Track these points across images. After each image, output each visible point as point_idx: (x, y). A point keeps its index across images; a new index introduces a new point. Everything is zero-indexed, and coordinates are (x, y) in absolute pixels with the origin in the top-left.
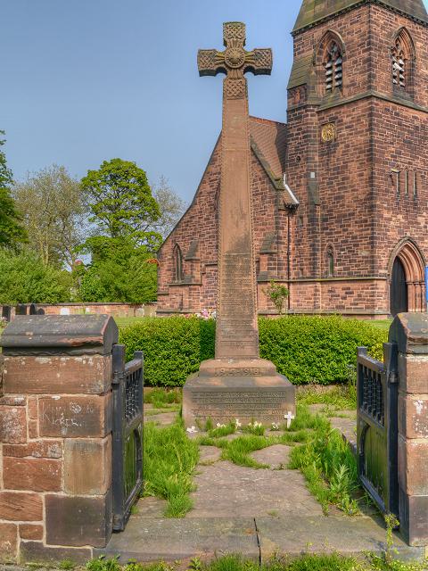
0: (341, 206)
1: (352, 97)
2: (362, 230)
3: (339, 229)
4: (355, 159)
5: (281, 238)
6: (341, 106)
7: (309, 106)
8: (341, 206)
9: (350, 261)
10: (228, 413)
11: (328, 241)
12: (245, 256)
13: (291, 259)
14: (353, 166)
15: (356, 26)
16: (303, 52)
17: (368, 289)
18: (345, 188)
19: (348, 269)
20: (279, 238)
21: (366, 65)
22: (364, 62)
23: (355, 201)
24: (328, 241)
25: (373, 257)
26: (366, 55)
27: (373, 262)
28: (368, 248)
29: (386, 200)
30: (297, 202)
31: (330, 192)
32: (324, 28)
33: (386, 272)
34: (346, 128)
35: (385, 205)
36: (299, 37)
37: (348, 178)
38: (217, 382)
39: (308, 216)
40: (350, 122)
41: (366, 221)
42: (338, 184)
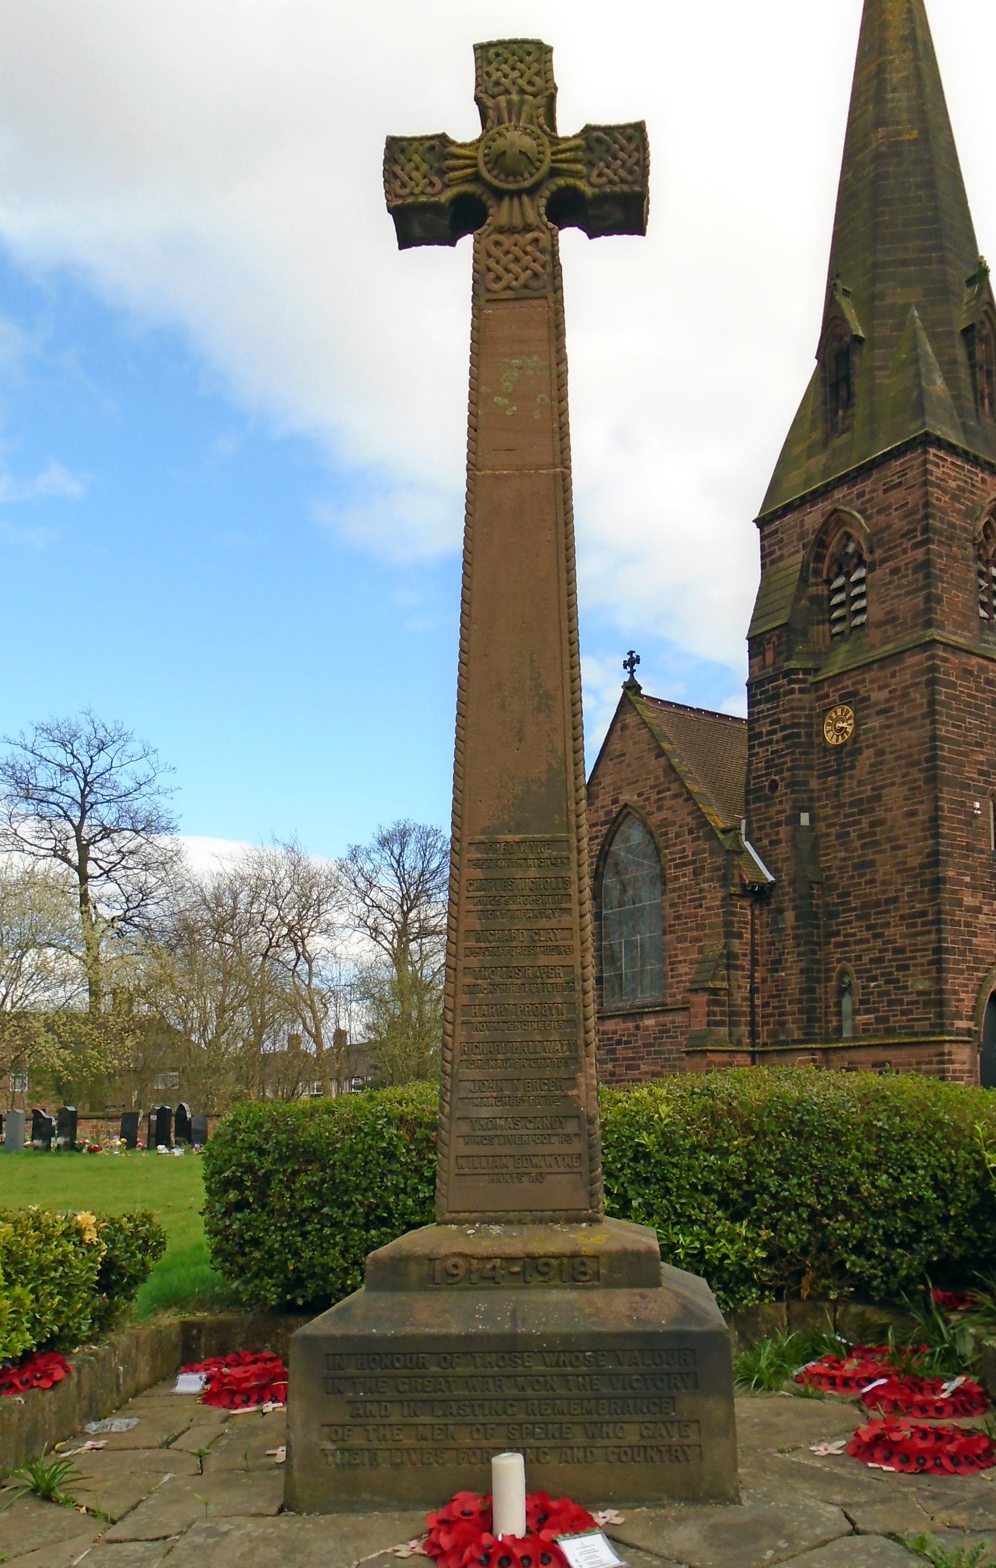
0: (867, 883)
1: (889, 647)
2: (916, 935)
3: (866, 934)
4: (898, 780)
5: (736, 956)
6: (866, 667)
7: (795, 671)
8: (867, 883)
9: (890, 1003)
10: (465, 1440)
11: (839, 961)
12: (548, 843)
13: (757, 1002)
14: (894, 795)
15: (895, 497)
16: (781, 558)
17: (930, 1063)
18: (875, 843)
19: (885, 1020)
20: (731, 955)
21: (920, 575)
22: (915, 571)
23: (898, 872)
24: (839, 961)
25: (941, 991)
26: (919, 554)
27: (941, 1003)
28: (929, 971)
29: (967, 867)
30: (771, 878)
31: (843, 855)
32: (825, 506)
33: (971, 1024)
34: (879, 713)
35: (967, 879)
36: (773, 527)
37: (881, 822)
38: (436, 1316)
39: (795, 908)
40: (887, 700)
41: (923, 913)
42: (860, 837)
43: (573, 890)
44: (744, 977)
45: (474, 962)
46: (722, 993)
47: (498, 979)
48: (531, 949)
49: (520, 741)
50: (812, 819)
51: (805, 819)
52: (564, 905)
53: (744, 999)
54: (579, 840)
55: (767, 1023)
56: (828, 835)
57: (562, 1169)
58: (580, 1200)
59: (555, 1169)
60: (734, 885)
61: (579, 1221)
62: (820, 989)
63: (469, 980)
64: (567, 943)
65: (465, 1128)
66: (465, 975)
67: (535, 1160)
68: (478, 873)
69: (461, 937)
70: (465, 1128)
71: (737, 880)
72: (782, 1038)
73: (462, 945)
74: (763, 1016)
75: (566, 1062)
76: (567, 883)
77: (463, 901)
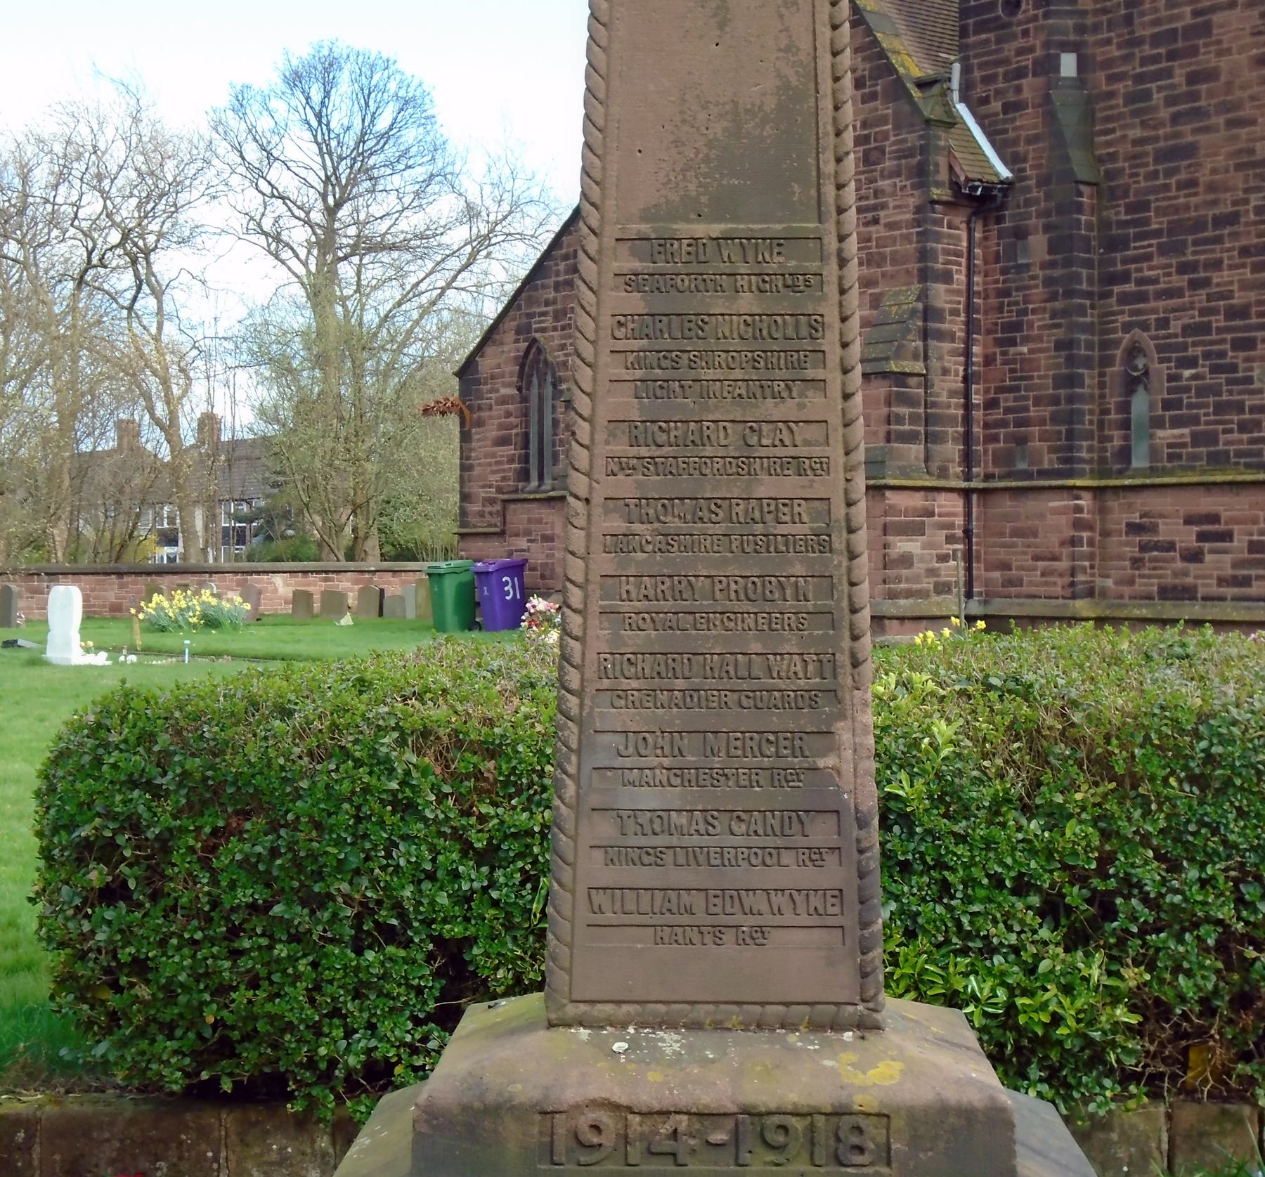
0: (1181, 186)
3: (1180, 281)
8: (1181, 186)
9: (1220, 408)
11: (1127, 327)
12: (778, 242)
13: (976, 399)
18: (1198, 113)
19: (1211, 438)
20: (929, 313)
23: (1239, 167)
24: (1127, 327)
30: (1005, 173)
31: (1137, 133)
37: (1211, 75)
39: (1047, 228)
42: (1170, 101)
43: (830, 342)
44: (953, 353)
45: (626, 486)
46: (913, 381)
47: (675, 524)
48: (744, 463)
49: (722, 25)
50: (1082, 65)
51: (1068, 65)
52: (810, 373)
53: (952, 394)
54: (842, 238)
55: (995, 439)
56: (1111, 95)
57: (804, 919)
58: (842, 985)
59: (788, 918)
60: (938, 184)
61: (837, 1026)
62: (1089, 378)
63: (616, 524)
64: (816, 451)
65: (605, 829)
66: (607, 512)
67: (748, 900)
68: (635, 303)
69: (600, 436)
70: (605, 829)
71: (943, 176)
72: (1022, 466)
73: (602, 450)
74: (986, 425)
75: (811, 698)
76: (816, 326)
77: (605, 358)
